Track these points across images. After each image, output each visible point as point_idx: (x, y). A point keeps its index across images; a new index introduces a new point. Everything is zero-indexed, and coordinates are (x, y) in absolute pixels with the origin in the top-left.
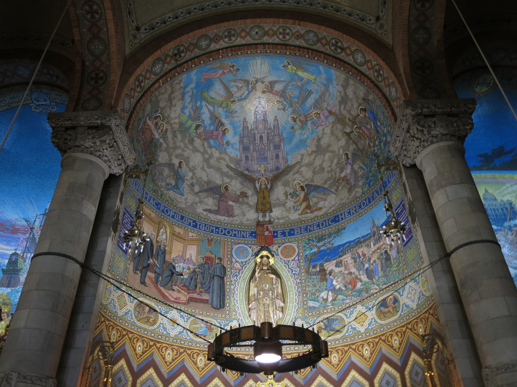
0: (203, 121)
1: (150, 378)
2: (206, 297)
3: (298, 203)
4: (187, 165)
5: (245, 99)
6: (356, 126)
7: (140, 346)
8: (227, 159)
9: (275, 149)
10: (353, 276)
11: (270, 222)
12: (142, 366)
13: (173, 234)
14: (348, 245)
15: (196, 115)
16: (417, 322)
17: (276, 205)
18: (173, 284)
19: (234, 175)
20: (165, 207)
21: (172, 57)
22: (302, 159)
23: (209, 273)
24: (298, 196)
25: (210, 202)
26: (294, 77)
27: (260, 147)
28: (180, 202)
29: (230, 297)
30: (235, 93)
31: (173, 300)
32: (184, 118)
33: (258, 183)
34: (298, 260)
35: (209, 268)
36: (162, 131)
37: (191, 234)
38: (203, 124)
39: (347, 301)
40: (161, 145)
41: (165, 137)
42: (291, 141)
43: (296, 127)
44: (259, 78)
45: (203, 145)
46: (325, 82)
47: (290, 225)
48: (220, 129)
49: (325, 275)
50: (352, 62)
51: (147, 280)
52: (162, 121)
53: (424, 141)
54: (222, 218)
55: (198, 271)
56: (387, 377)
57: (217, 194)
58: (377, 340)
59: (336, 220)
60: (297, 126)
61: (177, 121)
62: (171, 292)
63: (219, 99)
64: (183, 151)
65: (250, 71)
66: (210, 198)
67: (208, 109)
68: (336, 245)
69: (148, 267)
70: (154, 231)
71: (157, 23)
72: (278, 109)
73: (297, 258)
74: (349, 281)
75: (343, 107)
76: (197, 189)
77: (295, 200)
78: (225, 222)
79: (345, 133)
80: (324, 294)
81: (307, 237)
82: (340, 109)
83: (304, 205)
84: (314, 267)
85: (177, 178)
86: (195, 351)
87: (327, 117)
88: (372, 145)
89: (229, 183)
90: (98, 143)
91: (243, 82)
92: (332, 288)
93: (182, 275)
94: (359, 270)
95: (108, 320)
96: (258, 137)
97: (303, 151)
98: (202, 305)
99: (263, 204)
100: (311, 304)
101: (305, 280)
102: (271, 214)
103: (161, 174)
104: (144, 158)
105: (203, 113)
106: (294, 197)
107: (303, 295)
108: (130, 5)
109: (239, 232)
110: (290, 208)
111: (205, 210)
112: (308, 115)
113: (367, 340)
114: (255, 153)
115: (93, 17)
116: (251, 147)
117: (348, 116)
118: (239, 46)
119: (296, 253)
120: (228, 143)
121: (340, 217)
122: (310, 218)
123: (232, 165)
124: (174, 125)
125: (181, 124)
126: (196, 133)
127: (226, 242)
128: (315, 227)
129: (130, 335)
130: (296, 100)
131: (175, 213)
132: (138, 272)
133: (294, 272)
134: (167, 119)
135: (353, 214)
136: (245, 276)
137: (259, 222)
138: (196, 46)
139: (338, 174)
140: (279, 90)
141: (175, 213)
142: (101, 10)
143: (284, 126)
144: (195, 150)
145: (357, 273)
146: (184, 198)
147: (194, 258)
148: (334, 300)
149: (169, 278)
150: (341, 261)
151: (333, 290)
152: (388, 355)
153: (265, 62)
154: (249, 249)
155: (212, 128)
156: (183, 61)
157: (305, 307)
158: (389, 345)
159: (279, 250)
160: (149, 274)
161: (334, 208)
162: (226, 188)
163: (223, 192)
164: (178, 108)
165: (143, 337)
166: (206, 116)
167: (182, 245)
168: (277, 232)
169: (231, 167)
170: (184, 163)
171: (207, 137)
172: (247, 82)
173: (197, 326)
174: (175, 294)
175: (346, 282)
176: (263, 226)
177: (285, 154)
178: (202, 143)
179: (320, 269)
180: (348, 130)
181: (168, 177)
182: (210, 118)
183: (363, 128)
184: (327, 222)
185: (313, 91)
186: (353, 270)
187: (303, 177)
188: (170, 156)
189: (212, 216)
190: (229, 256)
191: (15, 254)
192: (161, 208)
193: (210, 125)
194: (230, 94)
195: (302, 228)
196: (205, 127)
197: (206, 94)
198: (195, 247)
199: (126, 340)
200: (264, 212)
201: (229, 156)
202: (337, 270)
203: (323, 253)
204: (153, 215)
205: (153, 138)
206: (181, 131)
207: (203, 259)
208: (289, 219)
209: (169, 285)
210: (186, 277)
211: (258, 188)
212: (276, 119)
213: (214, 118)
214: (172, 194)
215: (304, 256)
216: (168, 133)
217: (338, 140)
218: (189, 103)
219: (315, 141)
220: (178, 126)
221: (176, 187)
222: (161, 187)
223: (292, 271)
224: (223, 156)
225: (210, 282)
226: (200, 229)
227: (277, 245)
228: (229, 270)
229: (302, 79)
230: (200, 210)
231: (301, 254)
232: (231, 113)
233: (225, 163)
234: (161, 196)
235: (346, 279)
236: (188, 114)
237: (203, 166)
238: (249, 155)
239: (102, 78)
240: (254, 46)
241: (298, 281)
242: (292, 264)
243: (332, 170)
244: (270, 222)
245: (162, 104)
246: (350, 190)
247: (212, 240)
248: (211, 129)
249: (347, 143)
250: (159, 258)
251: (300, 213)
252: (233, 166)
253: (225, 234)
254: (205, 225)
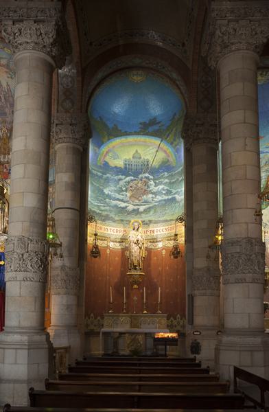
212: (8, 85)
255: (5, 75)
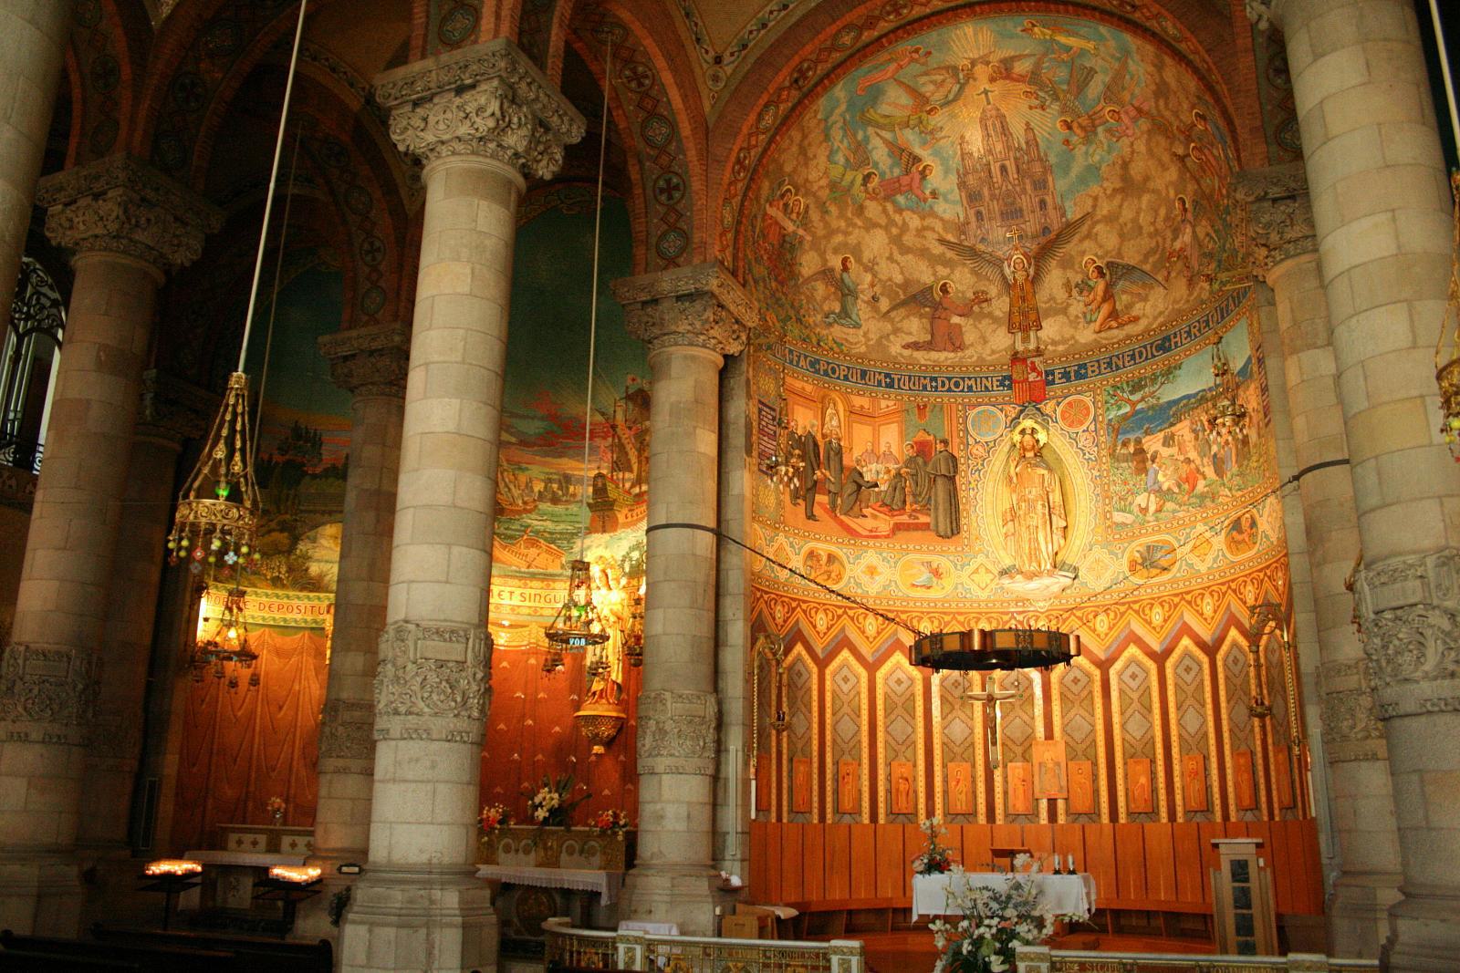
0: (876, 165)
1: (845, 665)
2: (923, 519)
3: (1093, 306)
4: (859, 260)
5: (955, 99)
6: (1193, 145)
7: (821, 619)
8: (938, 226)
9: (1035, 189)
10: (1193, 466)
11: (1039, 352)
12: (829, 648)
13: (851, 412)
14: (1185, 401)
15: (860, 155)
16: (1276, 568)
17: (1047, 316)
18: (863, 505)
19: (956, 258)
20: (828, 364)
21: (789, 88)
22: (1094, 207)
23: (925, 471)
24: (1093, 288)
25: (915, 327)
26: (1050, 47)
27: (1004, 188)
28: (858, 343)
29: (968, 513)
30: (933, 94)
31: (867, 533)
32: (835, 172)
33: (1009, 266)
34: (1096, 431)
35: (925, 463)
36: (798, 213)
37: (883, 403)
38: (877, 168)
39: (1181, 514)
40: (801, 240)
41: (805, 221)
42: (1066, 171)
43: (1074, 139)
44: (976, 56)
45: (885, 211)
46: (1118, 55)
47: (1077, 356)
48: (914, 169)
49: (1144, 461)
50: (1158, 30)
51: (817, 511)
52: (796, 195)
53: (1275, 249)
54: (942, 356)
55: (907, 473)
56: (1235, 652)
57: (926, 306)
58: (1224, 588)
59: (1164, 346)
60: (1076, 138)
61: (823, 182)
62: (861, 520)
63: (899, 114)
64: (846, 234)
65: (955, 48)
66: (912, 318)
67: (881, 137)
68: (1164, 400)
69: (814, 487)
70: (815, 417)
71: (751, 32)
72: (1031, 108)
73: (1092, 427)
74: (1184, 476)
75: (1161, 103)
76: (884, 304)
77: (1087, 300)
78: (949, 362)
79: (1175, 155)
80: (1141, 500)
81: (1111, 381)
82: (1157, 106)
83: (1106, 308)
84: (1125, 444)
85: (844, 295)
86: (914, 614)
87: (1134, 120)
88: (1224, 192)
89: (948, 277)
90: (698, 325)
91: (944, 72)
92: (1156, 487)
93: (876, 485)
94: (1202, 455)
95: (767, 593)
96: (995, 169)
97: (1095, 189)
98: (918, 534)
99: (1025, 315)
100: (1119, 517)
101: (1108, 471)
102: (1039, 333)
103: (811, 298)
104: (774, 284)
105: (873, 148)
106: (1085, 293)
107: (1104, 500)
108: (696, 24)
109: (979, 380)
110: (1077, 317)
111: (904, 347)
112: (1095, 113)
113: (1209, 587)
114: (995, 202)
115: (640, 84)
116: (986, 192)
117: (1176, 124)
118: (920, 19)
119: (1091, 417)
120: (934, 194)
121: (1173, 341)
122: (1115, 340)
123: (950, 238)
124: (819, 193)
125: (833, 186)
126: (866, 191)
127: (954, 406)
128: (1127, 359)
129: (804, 606)
130: (1065, 87)
131: (849, 368)
132: (800, 501)
133: (1087, 456)
134: (802, 188)
135: (1196, 337)
136: (995, 469)
137: (1016, 353)
138: (833, 48)
139: (1168, 241)
140: (1024, 73)
141: (849, 368)
142: (650, 70)
143: (1047, 139)
144: (871, 225)
145: (1198, 462)
146: (861, 332)
147: (894, 450)
148: (1159, 510)
149: (854, 497)
150: (1173, 435)
151: (1159, 491)
152: (1238, 615)
153: (981, 28)
154: (998, 412)
155: (897, 172)
156: (812, 82)
157: (1108, 523)
158: (1241, 599)
159: (1059, 410)
160: (819, 498)
161: (1161, 319)
162: (944, 289)
163: (938, 299)
164: (822, 159)
165: (824, 604)
166: (880, 153)
167: (871, 428)
168: (1053, 375)
169: (949, 242)
170: (852, 259)
171: (890, 191)
172: (953, 70)
173: (914, 571)
174: (869, 523)
175: (1180, 478)
176: (1024, 360)
177: (1058, 200)
178: (880, 208)
179: (1135, 450)
180: (1180, 151)
181: (826, 299)
182: (889, 155)
183: (1206, 151)
184: (1148, 347)
185: (1098, 70)
186: (1193, 455)
187: (1101, 247)
188: (822, 255)
189: (921, 357)
190: (961, 434)
191: (600, 476)
192: (822, 368)
193: (891, 168)
194: (921, 100)
195: (1101, 362)
196: (883, 174)
197: (872, 114)
198: (894, 427)
199: (799, 614)
200: (1025, 329)
201: (942, 219)
202: (1165, 452)
203: (1140, 416)
204: (809, 388)
205: (784, 236)
206: (835, 199)
207: (912, 447)
208: (1076, 341)
209: (856, 508)
210: (883, 487)
211: (1010, 278)
212: (1028, 128)
213: (898, 151)
214: (837, 331)
215: (1106, 422)
216: (810, 212)
217: (1164, 168)
218: (841, 142)
219: (1117, 167)
220: (827, 191)
221: (845, 313)
222: (816, 325)
223: (1084, 454)
224: (928, 221)
225: (930, 489)
226: (899, 388)
227: (1055, 401)
228: (962, 461)
229: (1068, 49)
230: (895, 348)
231: (1101, 418)
232: (931, 132)
233: (936, 236)
234: (818, 344)
235: (1180, 471)
236: (842, 161)
237: (891, 254)
238: (982, 208)
239: (677, 188)
240: (950, 13)
241: (1096, 473)
242: (1082, 440)
243: (1156, 230)
244: (1039, 352)
245: (788, 168)
246: (1191, 283)
247: (925, 406)
248: (895, 175)
249: (1181, 177)
250: (832, 466)
251: (1097, 329)
252: (952, 240)
253: (949, 390)
254: (910, 377)
255: (1023, 105)
